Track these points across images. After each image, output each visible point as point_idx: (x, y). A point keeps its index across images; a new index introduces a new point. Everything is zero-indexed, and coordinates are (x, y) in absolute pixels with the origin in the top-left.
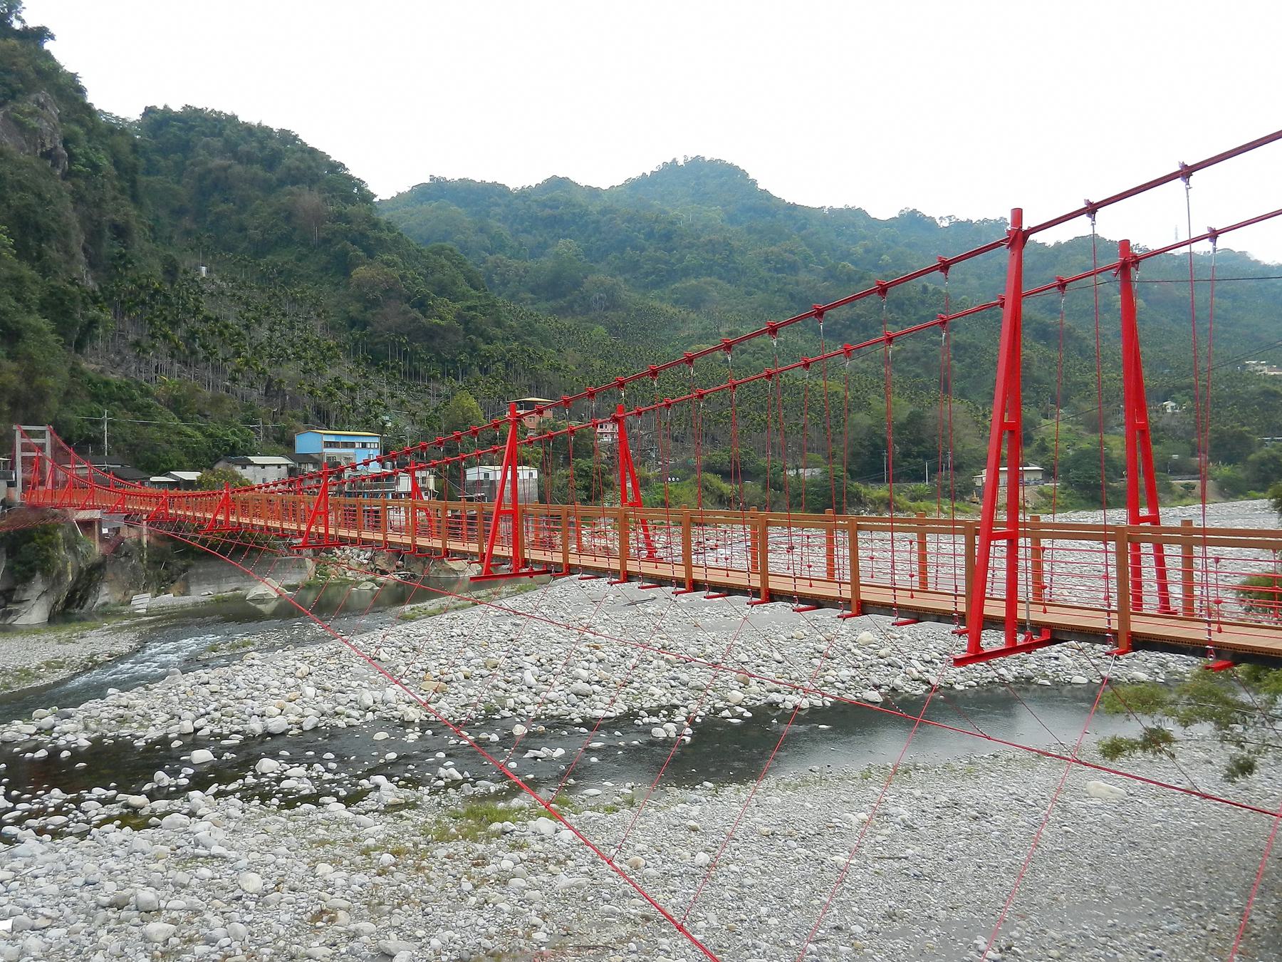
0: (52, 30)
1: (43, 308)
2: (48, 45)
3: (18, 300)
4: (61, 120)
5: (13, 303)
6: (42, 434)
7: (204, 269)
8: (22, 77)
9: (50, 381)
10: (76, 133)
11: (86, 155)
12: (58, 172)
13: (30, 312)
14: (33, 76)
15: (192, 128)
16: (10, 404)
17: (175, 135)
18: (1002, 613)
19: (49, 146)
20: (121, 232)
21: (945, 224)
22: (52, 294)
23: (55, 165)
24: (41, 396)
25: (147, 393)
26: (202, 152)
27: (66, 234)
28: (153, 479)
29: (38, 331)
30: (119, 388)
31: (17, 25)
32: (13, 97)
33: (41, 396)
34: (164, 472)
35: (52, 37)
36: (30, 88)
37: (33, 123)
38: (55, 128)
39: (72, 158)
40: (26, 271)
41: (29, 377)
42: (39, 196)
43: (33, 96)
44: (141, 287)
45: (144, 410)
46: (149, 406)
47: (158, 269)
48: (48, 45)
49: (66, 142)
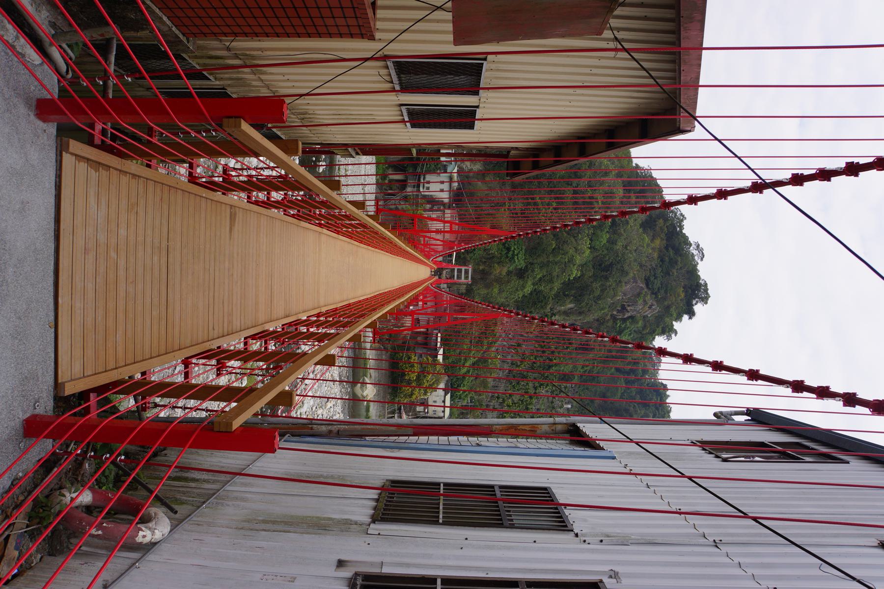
0: (694, 319)
1: (536, 292)
2: (686, 317)
3: (540, 279)
4: (644, 317)
5: (538, 277)
6: (467, 278)
7: (569, 406)
8: (664, 299)
9: (496, 290)
10: (637, 323)
11: (625, 329)
12: (615, 313)
13: (533, 284)
14: (666, 303)
15: (657, 409)
16: (483, 270)
17: (651, 399)
18: (335, 411)
19: (628, 308)
20: (585, 348)
21: (702, 282)
22: (545, 298)
23: (618, 311)
24: (488, 286)
25: (490, 345)
26: (643, 412)
27: (580, 313)
28: (439, 335)
29: (523, 287)
30: (493, 331)
31: (694, 302)
32: (653, 293)
33: (488, 286)
34: (444, 342)
35: (690, 318)
36: (658, 302)
37: (640, 301)
38: (638, 312)
39: (624, 320)
40: (557, 285)
41: (499, 280)
42: (599, 298)
43: (655, 303)
44: (553, 352)
45: (479, 342)
46: (482, 346)
47: (567, 369)
48: (686, 317)
49: (632, 317)
